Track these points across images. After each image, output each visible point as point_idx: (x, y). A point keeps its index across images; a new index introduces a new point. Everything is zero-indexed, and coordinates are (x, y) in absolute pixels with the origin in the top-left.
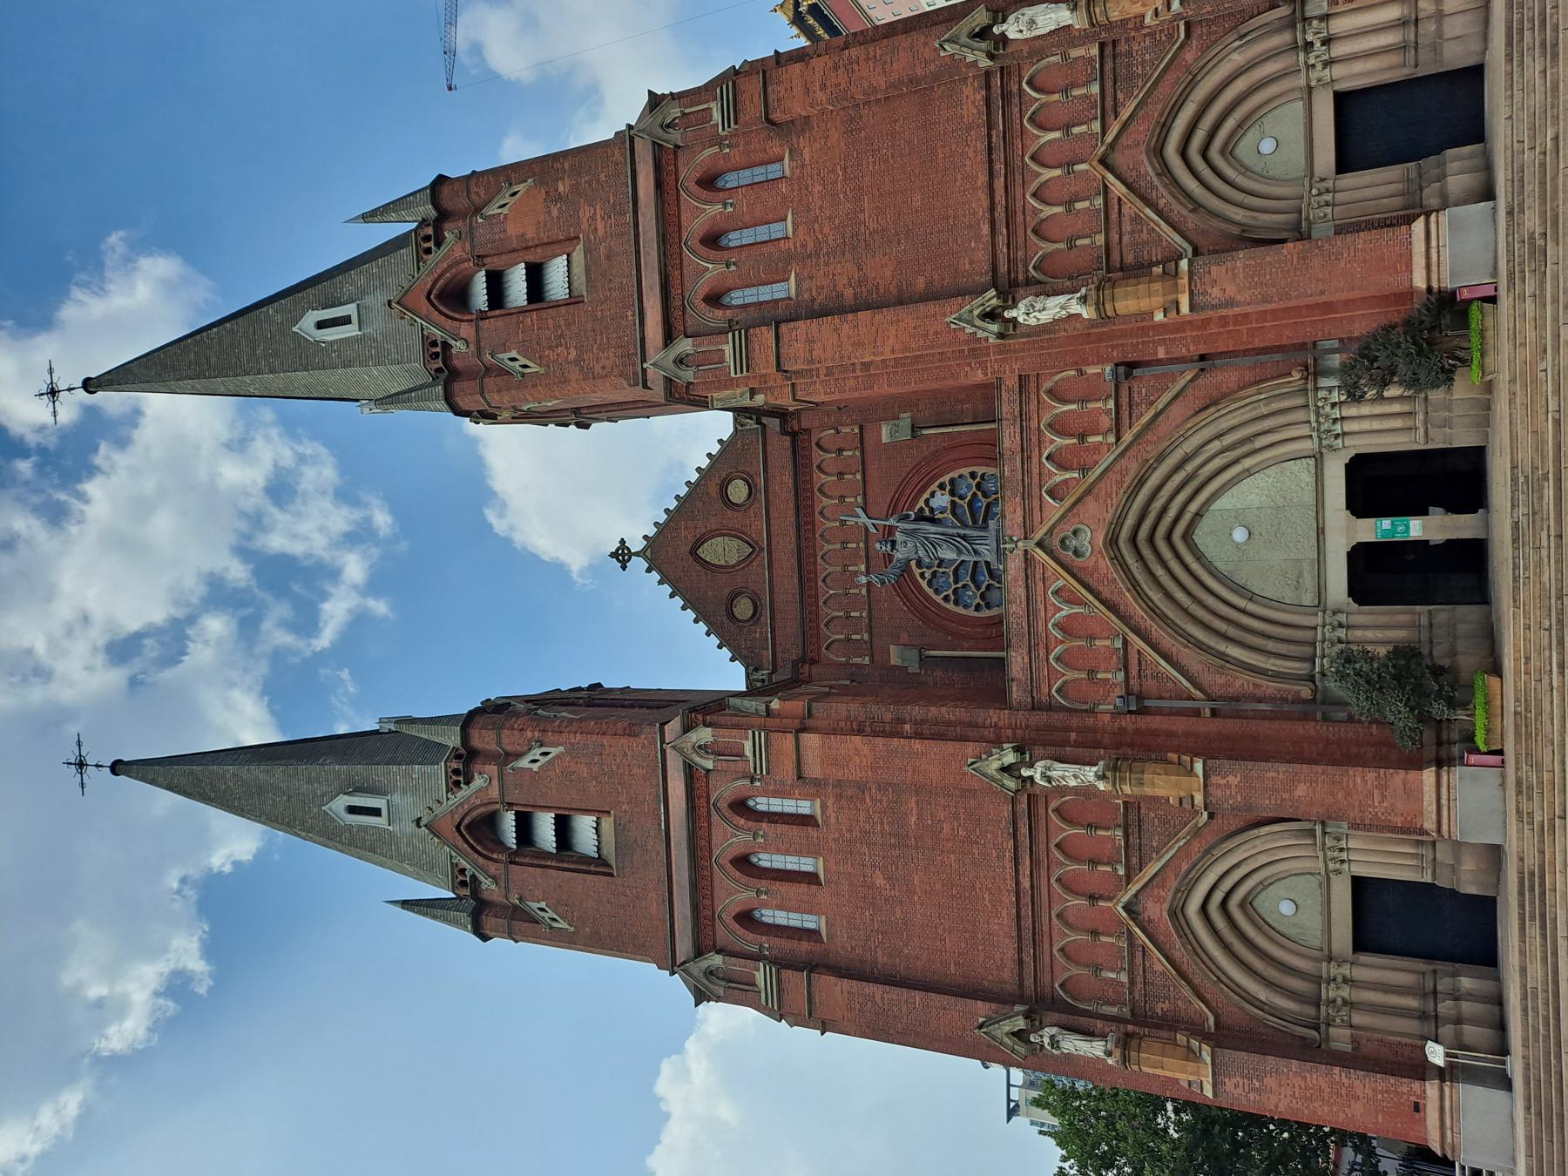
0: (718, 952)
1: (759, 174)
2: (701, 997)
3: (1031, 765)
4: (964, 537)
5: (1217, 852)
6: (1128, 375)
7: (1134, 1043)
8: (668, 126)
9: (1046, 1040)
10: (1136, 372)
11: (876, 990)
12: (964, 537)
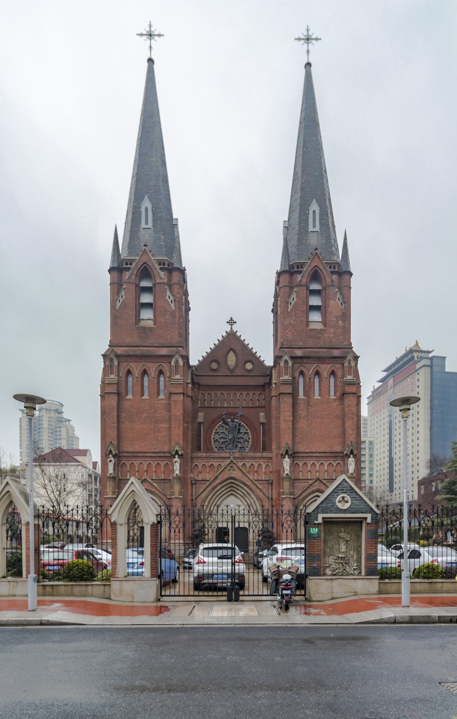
0: (118, 363)
1: (332, 389)
2: (104, 356)
3: (178, 458)
4: (234, 441)
5: (161, 500)
6: (269, 483)
7: (114, 480)
8: (349, 362)
9: (111, 459)
10: (270, 485)
11: (115, 413)
12: (234, 441)
